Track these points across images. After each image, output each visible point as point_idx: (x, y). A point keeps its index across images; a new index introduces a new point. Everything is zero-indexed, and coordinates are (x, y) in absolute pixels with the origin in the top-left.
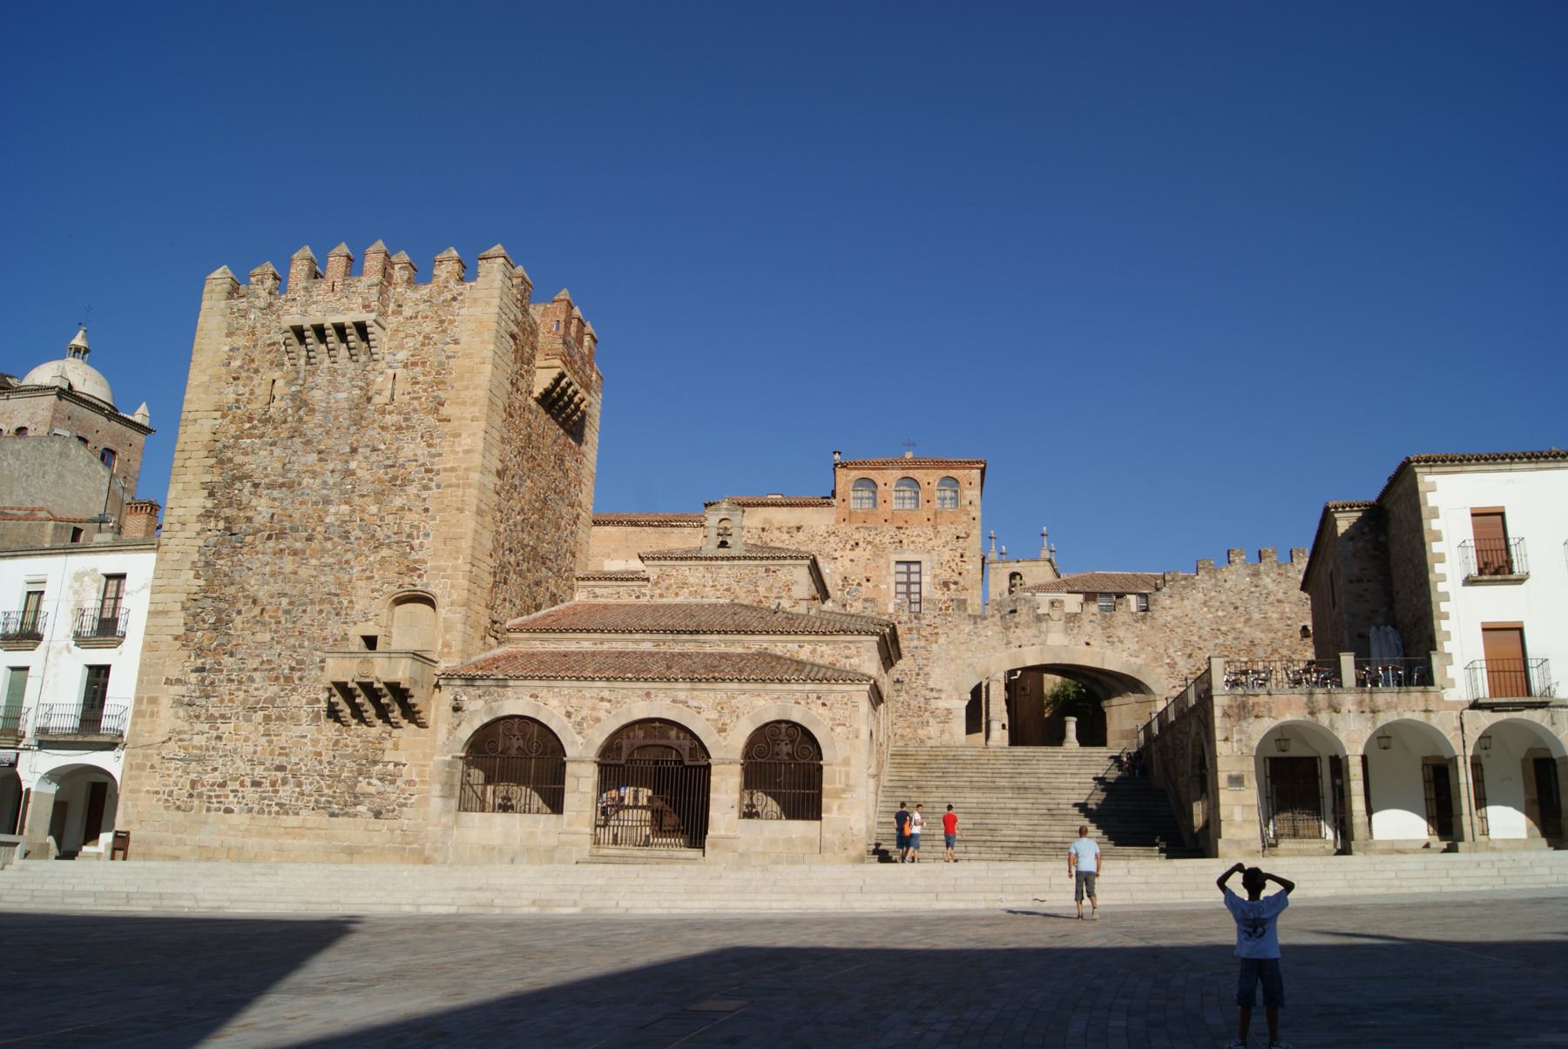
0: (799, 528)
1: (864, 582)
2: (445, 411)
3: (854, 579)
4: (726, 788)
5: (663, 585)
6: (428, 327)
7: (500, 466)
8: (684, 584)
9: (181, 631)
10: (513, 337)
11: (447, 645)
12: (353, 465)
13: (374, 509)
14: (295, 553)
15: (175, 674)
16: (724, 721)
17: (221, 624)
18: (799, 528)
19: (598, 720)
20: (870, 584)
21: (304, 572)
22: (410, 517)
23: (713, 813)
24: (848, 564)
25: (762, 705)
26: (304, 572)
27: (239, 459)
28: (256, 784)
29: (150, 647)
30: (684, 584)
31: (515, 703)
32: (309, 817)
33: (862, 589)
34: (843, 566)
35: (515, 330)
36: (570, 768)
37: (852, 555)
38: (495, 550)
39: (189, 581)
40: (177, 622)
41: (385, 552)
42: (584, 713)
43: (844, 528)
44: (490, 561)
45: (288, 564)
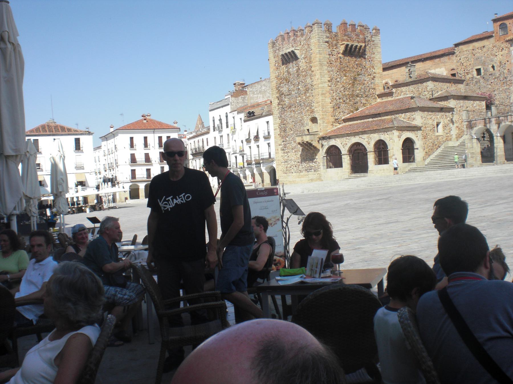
0: (484, 47)
1: (507, 63)
2: (313, 69)
3: (503, 62)
4: (371, 158)
5: (397, 93)
6: (306, 47)
7: (329, 79)
8: (402, 92)
9: (279, 133)
10: (327, 42)
11: (320, 129)
12: (299, 87)
13: (304, 97)
14: (294, 111)
15: (280, 143)
16: (369, 142)
17: (285, 131)
18: (484, 47)
19: (346, 144)
20: (508, 63)
21: (296, 115)
22: (310, 98)
23: (369, 164)
24: (501, 57)
25: (376, 137)
26: (296, 115)
27: (281, 89)
28: (296, 166)
29: (275, 138)
30: (402, 92)
31: (332, 142)
32: (304, 173)
33: (506, 65)
34: (499, 58)
35: (327, 40)
36: (343, 156)
37: (501, 53)
38: (332, 101)
39: (278, 121)
40: (278, 131)
41: (308, 108)
42: (344, 142)
43: (498, 44)
44: (331, 105)
45: (293, 114)
